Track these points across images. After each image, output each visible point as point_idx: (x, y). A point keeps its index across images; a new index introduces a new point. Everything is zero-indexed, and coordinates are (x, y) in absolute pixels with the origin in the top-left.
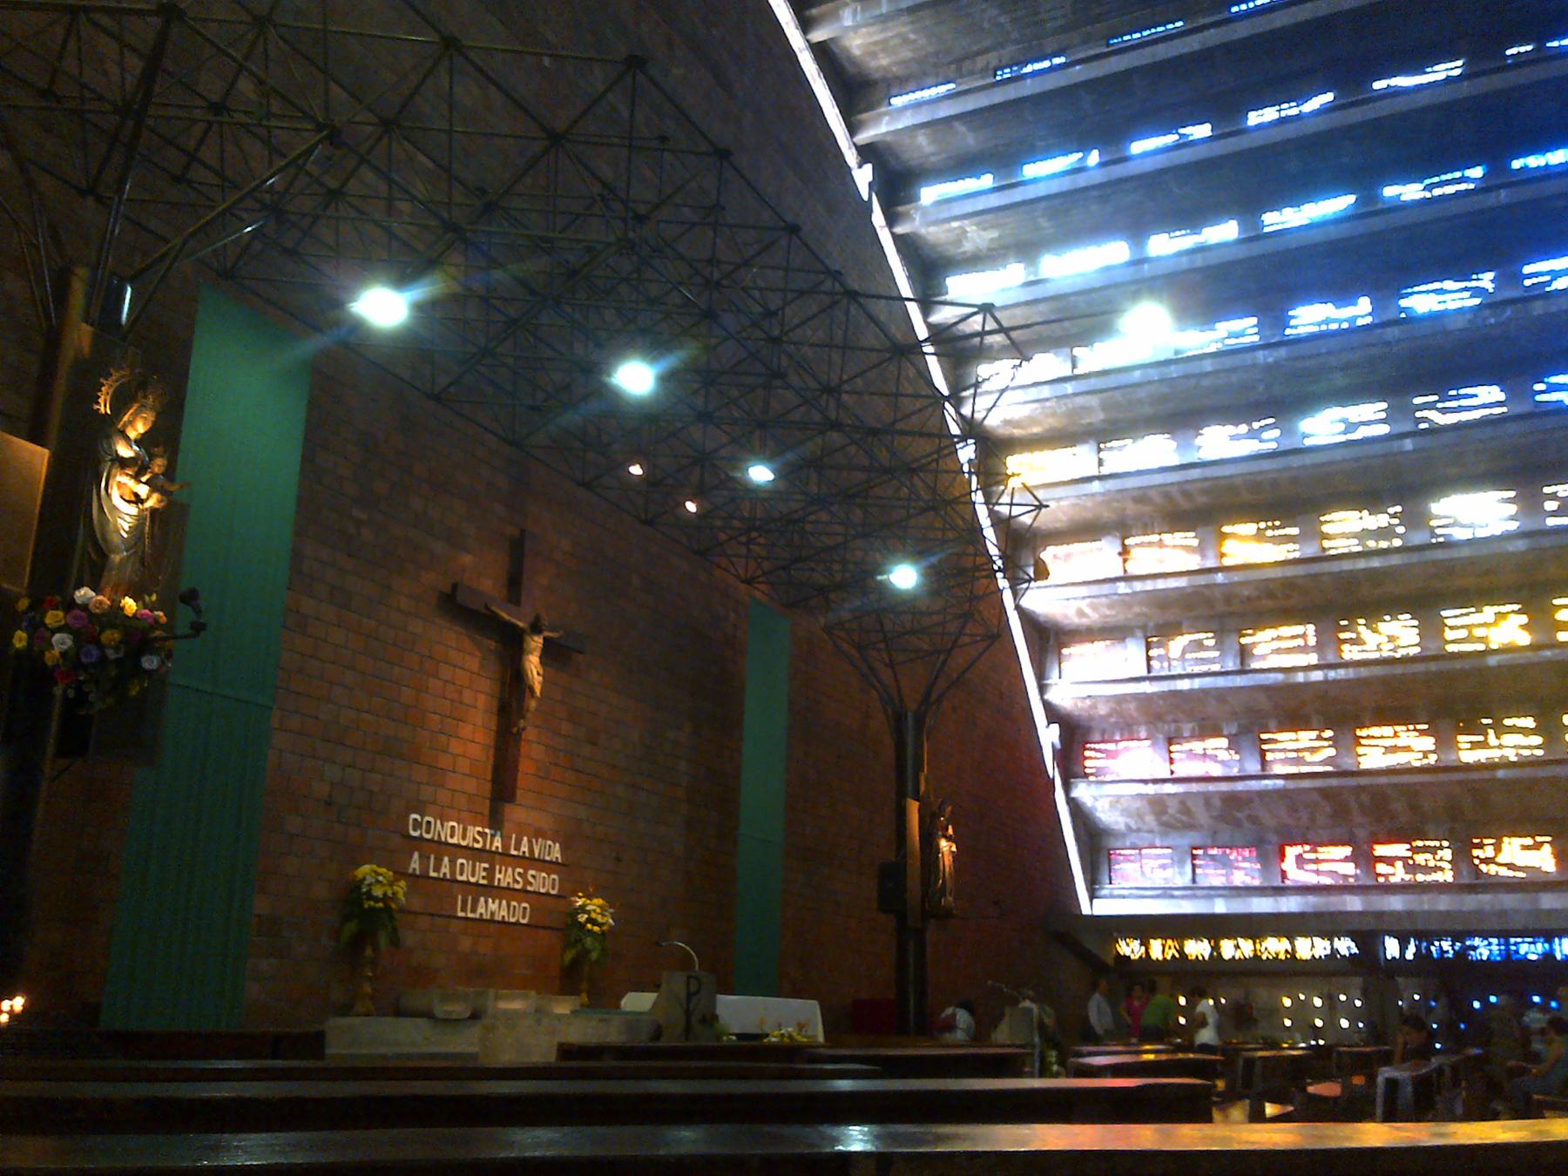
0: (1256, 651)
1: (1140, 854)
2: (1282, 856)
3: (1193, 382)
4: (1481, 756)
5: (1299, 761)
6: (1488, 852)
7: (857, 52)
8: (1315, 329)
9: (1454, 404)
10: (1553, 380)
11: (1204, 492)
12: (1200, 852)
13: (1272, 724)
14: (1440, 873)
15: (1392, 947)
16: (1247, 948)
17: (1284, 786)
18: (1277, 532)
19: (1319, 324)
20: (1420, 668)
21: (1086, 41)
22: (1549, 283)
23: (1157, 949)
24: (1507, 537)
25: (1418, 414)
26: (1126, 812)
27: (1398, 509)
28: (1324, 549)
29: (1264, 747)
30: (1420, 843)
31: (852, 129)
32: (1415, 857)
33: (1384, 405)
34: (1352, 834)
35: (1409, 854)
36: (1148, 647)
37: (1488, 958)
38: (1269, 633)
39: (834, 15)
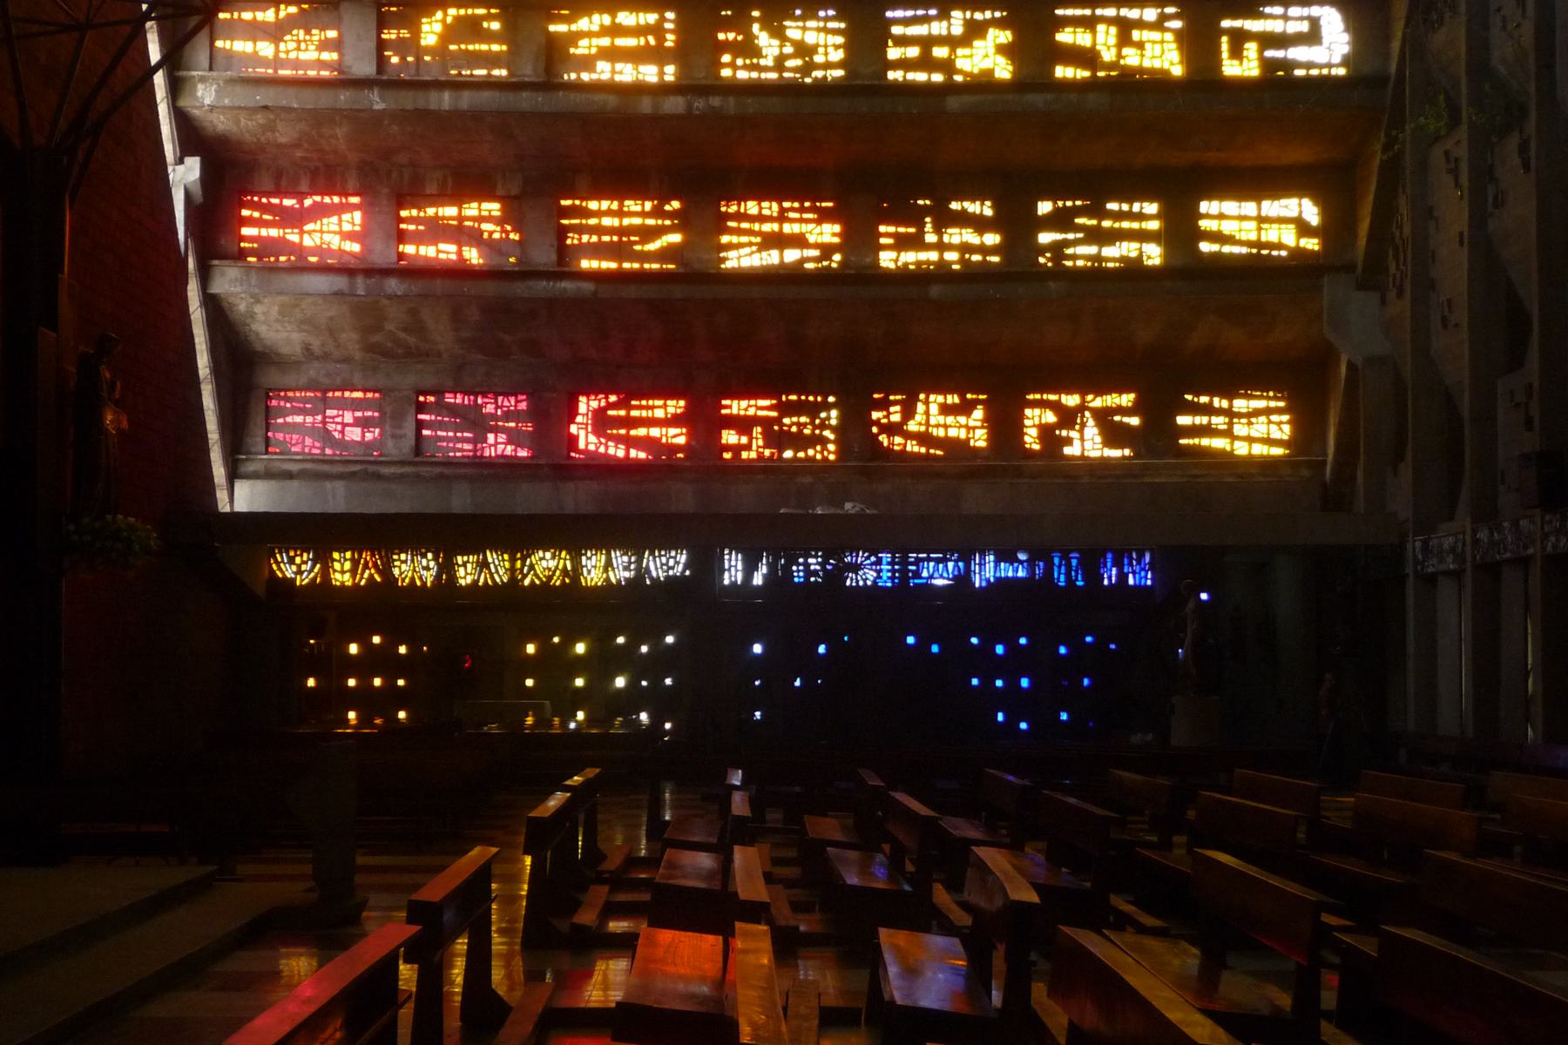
1: (324, 399)
2: (573, 413)
4: (910, 257)
5: (618, 251)
15: (733, 569)
16: (499, 567)
17: (596, 292)
26: (307, 323)
32: (786, 421)
35: (774, 414)
37: (875, 582)
38: (599, 20)
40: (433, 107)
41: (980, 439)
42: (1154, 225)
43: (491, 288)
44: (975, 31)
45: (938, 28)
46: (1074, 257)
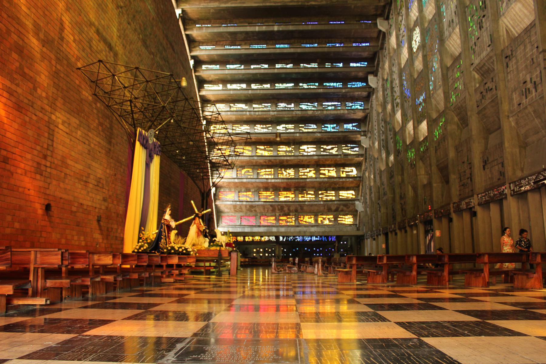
0: (262, 174)
2: (260, 219)
4: (303, 199)
6: (302, 219)
10: (326, 125)
11: (255, 139)
13: (262, 190)
15: (281, 238)
19: (282, 107)
20: (294, 180)
21: (245, 44)
22: (327, 107)
24: (313, 155)
27: (294, 147)
28: (278, 154)
30: (289, 217)
33: (293, 125)
34: (275, 214)
36: (237, 171)
39: (192, 29)
41: (313, 222)
42: (334, 195)
43: (250, 203)
44: (310, 171)
45: (305, 171)
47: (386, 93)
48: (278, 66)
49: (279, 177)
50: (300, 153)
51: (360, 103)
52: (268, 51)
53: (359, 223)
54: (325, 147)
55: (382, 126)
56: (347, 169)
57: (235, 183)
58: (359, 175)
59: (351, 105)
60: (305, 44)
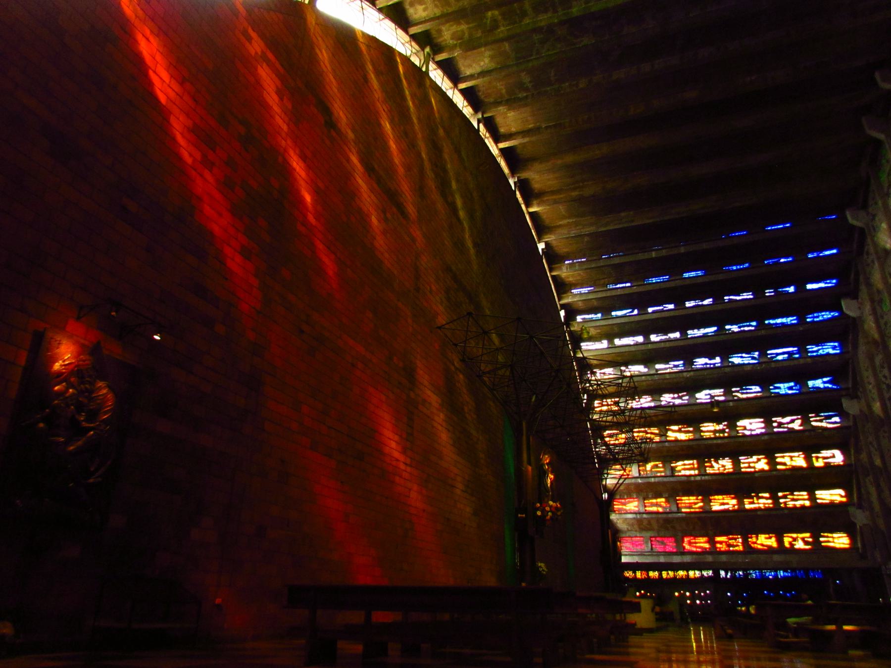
0: (678, 468)
2: (683, 541)
3: (661, 381)
4: (752, 506)
6: (754, 540)
7: (563, 277)
8: (702, 366)
9: (745, 391)
10: (776, 385)
12: (654, 539)
13: (681, 494)
14: (738, 547)
15: (722, 573)
16: (671, 573)
18: (685, 429)
20: (734, 477)
22: (775, 357)
23: (639, 574)
24: (762, 434)
25: (734, 394)
26: (628, 524)
27: (726, 423)
29: (678, 502)
30: (731, 536)
31: (559, 300)
32: (730, 541)
33: (722, 390)
35: (727, 540)
36: (639, 467)
39: (560, 268)
40: (650, 481)
41: (775, 545)
43: (664, 516)
44: (759, 460)
45: (750, 460)
46: (789, 504)
47: (882, 322)
48: (689, 304)
49: (708, 471)
50: (738, 433)
51: (832, 344)
52: (672, 284)
53: (864, 545)
54: (779, 419)
55: (885, 377)
56: (825, 453)
57: (637, 485)
58: (847, 462)
59: (816, 349)
60: (729, 266)
